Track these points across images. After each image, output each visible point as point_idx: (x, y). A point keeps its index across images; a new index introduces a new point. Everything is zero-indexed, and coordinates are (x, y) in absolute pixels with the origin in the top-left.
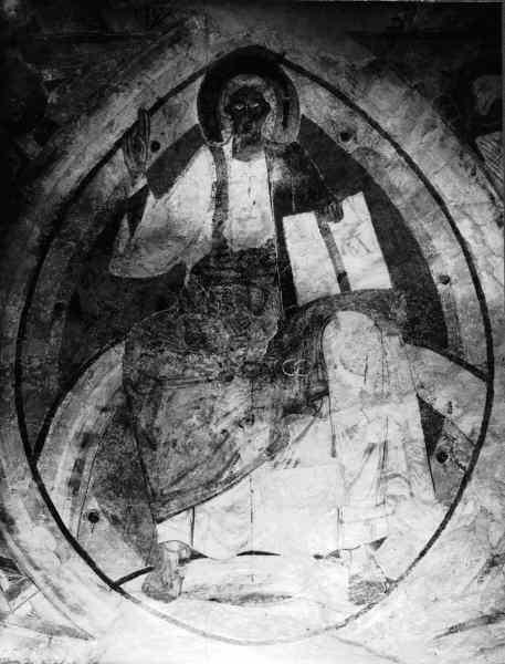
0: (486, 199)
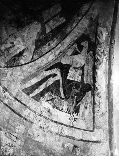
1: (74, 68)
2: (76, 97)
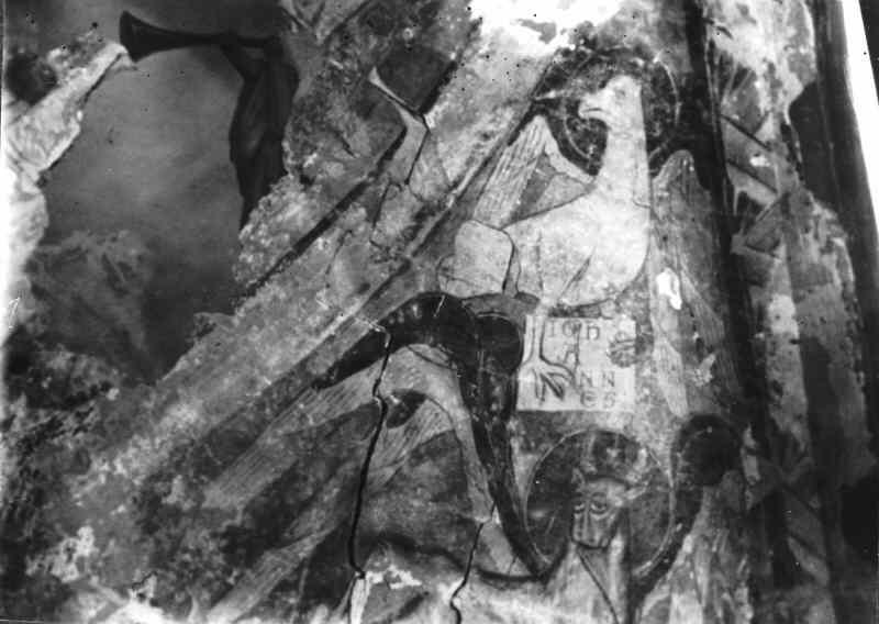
0: (452, 175)
1: (558, 312)
2: (618, 544)
